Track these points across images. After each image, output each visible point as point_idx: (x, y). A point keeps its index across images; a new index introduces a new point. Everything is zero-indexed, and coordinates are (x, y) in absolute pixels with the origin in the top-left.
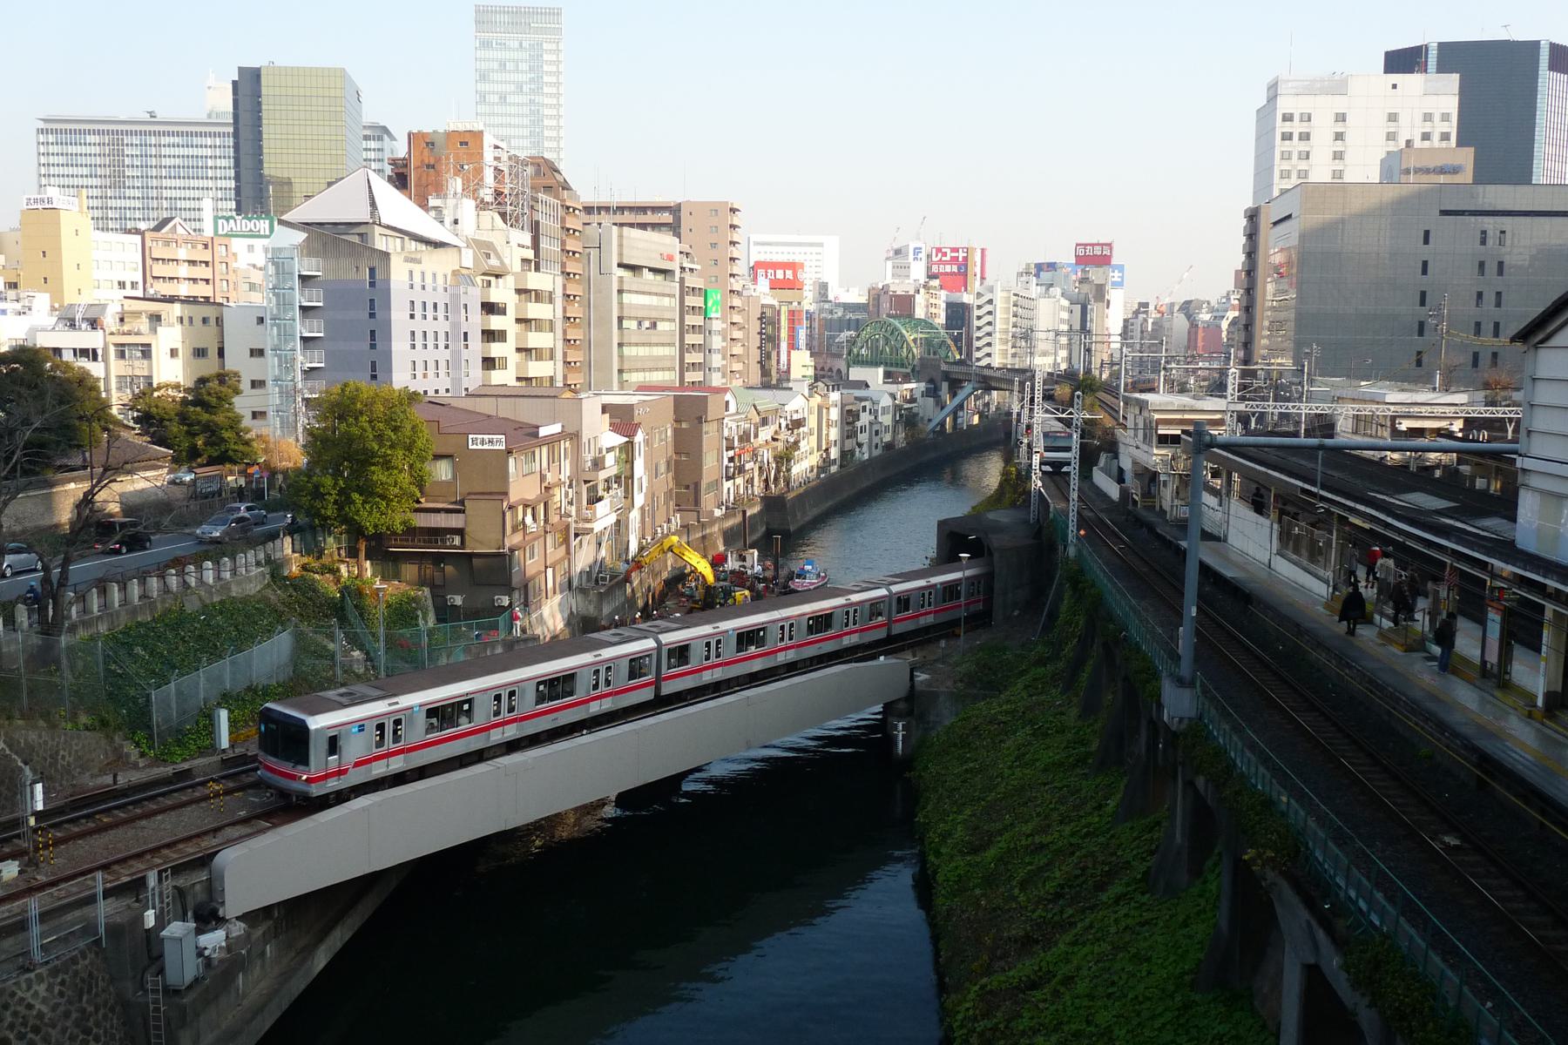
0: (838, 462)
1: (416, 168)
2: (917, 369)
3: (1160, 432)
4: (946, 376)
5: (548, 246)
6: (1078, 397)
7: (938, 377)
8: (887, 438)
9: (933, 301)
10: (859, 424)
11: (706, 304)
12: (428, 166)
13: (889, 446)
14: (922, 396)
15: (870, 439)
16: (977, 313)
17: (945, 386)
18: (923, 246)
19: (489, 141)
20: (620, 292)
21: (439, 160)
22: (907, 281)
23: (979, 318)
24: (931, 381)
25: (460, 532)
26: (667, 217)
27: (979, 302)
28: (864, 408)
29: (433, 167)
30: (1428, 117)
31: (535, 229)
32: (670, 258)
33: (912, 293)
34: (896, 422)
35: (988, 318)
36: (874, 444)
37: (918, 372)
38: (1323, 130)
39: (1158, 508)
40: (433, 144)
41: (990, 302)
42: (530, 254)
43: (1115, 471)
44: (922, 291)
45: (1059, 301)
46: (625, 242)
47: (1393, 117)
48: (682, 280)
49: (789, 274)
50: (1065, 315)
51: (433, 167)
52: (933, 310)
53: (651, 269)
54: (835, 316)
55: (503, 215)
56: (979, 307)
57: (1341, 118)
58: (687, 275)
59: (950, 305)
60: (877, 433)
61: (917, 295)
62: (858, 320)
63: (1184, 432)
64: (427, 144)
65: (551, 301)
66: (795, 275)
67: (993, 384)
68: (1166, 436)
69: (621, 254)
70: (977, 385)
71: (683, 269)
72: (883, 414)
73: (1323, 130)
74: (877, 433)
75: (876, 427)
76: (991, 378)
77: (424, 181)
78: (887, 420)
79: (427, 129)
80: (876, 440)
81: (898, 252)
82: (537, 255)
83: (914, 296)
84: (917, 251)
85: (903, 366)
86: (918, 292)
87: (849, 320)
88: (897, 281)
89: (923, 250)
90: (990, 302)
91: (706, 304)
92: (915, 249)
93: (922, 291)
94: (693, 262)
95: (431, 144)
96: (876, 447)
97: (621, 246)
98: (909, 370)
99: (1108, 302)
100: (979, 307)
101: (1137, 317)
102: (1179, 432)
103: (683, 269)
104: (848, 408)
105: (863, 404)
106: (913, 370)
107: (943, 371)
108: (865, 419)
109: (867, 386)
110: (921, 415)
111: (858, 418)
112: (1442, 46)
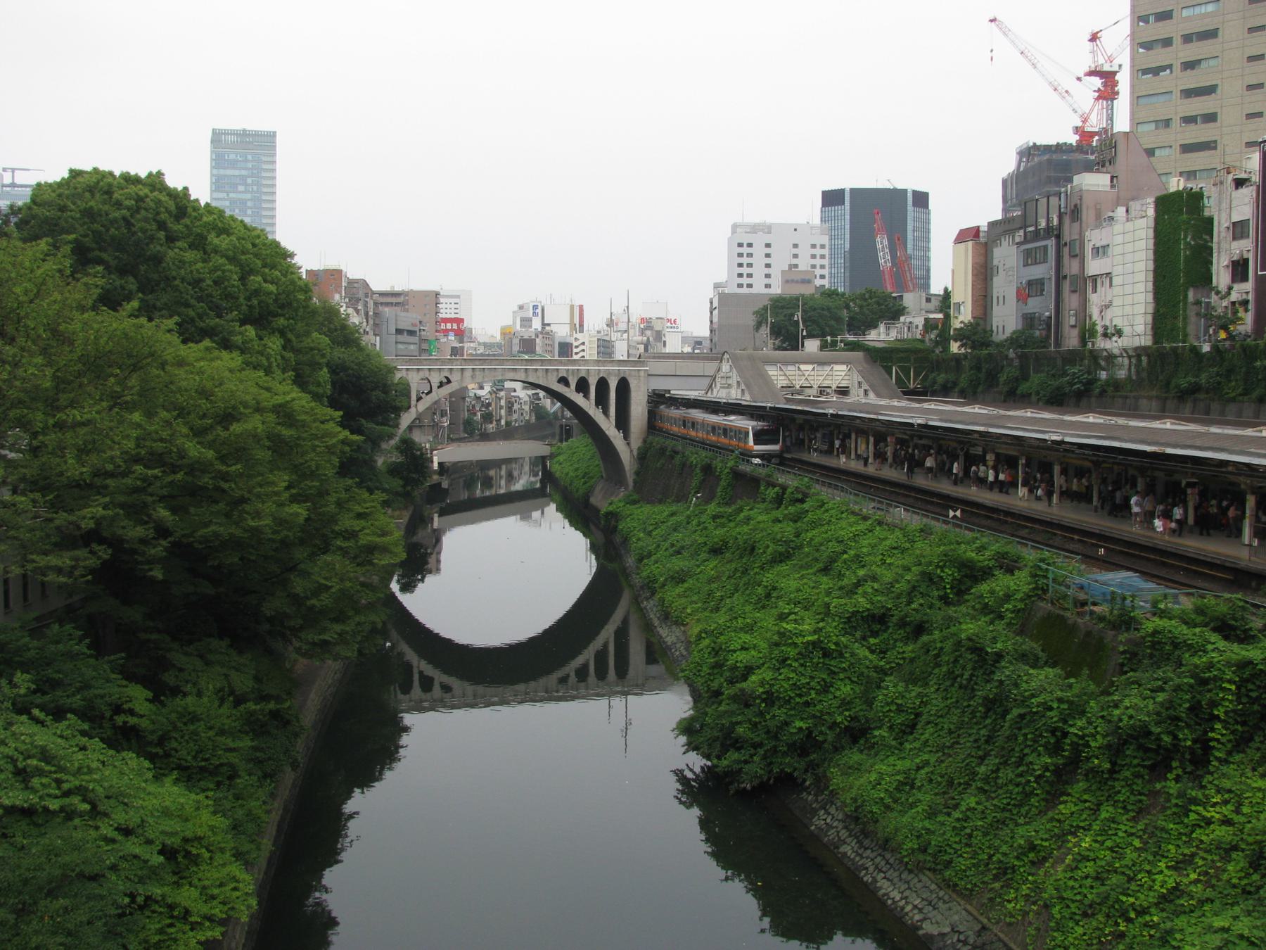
13: (528, 421)
16: (575, 350)
23: (576, 353)
26: (401, 299)
27: (575, 344)
30: (814, 246)
32: (414, 325)
34: (531, 410)
38: (759, 251)
41: (583, 344)
44: (540, 336)
47: (795, 246)
49: (455, 327)
54: (479, 352)
56: (577, 347)
57: (768, 245)
58: (423, 333)
66: (458, 326)
73: (759, 251)
78: (527, 408)
79: (315, 268)
81: (521, 307)
93: (540, 336)
99: (665, 342)
100: (577, 347)
108: (516, 407)
109: (515, 391)
111: (513, 405)
112: (852, 190)
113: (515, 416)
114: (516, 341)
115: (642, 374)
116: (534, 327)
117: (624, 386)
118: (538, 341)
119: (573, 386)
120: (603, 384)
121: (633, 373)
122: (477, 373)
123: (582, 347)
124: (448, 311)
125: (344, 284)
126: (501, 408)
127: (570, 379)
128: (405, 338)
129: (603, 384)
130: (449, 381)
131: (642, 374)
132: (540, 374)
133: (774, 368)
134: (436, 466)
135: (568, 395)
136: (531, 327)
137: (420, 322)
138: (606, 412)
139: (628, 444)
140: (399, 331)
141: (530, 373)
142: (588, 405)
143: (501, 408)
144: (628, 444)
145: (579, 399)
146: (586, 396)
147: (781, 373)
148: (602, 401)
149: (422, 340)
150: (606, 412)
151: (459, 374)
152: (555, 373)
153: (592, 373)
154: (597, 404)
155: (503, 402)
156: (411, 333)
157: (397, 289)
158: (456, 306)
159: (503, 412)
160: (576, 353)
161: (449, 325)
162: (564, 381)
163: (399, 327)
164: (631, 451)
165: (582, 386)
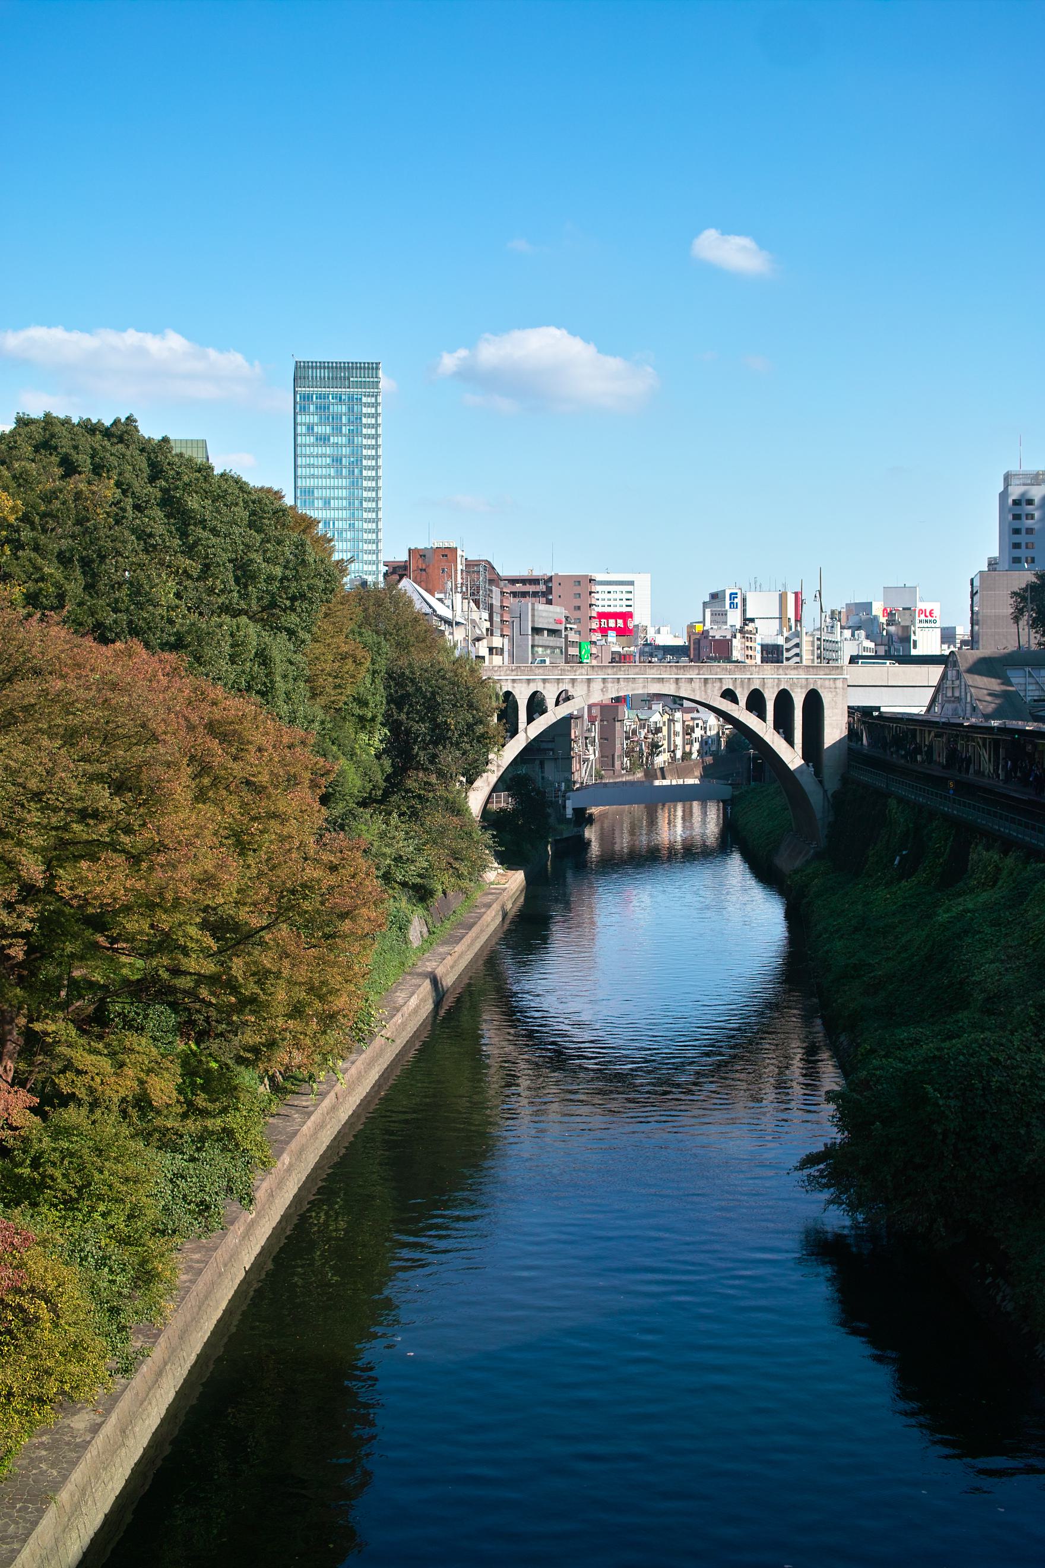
1: (413, 571)
5: (497, 619)
9: (749, 644)
11: (580, 652)
12: (421, 570)
16: (786, 655)
18: (739, 592)
19: (459, 552)
20: (533, 646)
21: (428, 566)
22: (725, 627)
23: (788, 659)
25: (552, 750)
26: (542, 587)
27: (786, 646)
28: (697, 725)
29: (425, 570)
31: (490, 609)
33: (729, 637)
40: (425, 556)
41: (797, 645)
42: (488, 624)
44: (738, 635)
45: (861, 643)
46: (536, 613)
48: (566, 636)
51: (425, 570)
52: (750, 653)
53: (549, 631)
55: (477, 603)
56: (788, 650)
59: (762, 646)
64: (421, 556)
65: (502, 654)
66: (625, 623)
69: (533, 621)
71: (566, 628)
77: (418, 580)
79: (421, 546)
81: (714, 596)
82: (492, 625)
83: (731, 640)
84: (733, 596)
88: (715, 627)
89: (739, 596)
91: (580, 652)
92: (731, 594)
93: (738, 635)
94: (570, 623)
95: (423, 556)
97: (533, 616)
99: (915, 642)
100: (788, 650)
103: (566, 628)
104: (686, 723)
105: (696, 722)
111: (693, 731)
115: (839, 684)
116: (729, 623)
117: (814, 701)
118: (735, 642)
119: (743, 701)
120: (784, 699)
121: (827, 682)
122: (610, 685)
124: (612, 603)
125: (460, 567)
126: (676, 734)
127: (738, 692)
128: (545, 639)
129: (784, 699)
130: (568, 699)
131: (839, 684)
132: (696, 685)
133: (1020, 673)
134: (569, 813)
135: (735, 715)
136: (725, 623)
137: (567, 618)
138: (790, 740)
139: (821, 782)
140: (536, 631)
141: (682, 684)
142: (765, 729)
143: (676, 734)
144: (821, 782)
145: (751, 720)
146: (762, 716)
147: (1031, 680)
148: (783, 725)
149: (568, 644)
150: (790, 740)
151: (585, 687)
152: (718, 685)
153: (769, 683)
154: (777, 727)
155: (678, 727)
156: (553, 632)
157: (537, 573)
158: (629, 596)
159: (679, 741)
160: (788, 659)
161: (612, 623)
162: (729, 695)
163: (536, 626)
164: (825, 791)
165: (756, 703)
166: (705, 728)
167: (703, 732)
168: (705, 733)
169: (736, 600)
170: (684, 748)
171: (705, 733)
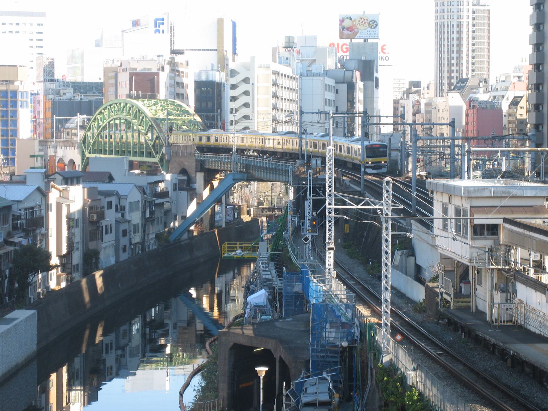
0: (81, 268)
2: (166, 158)
3: (476, 222)
4: (201, 166)
6: (388, 182)
7: (191, 166)
8: (137, 239)
10: (104, 223)
14: (175, 189)
15: (117, 240)
17: (200, 177)
24: (184, 172)
33: (154, 70)
35: (244, 99)
36: (122, 246)
37: (168, 161)
39: (473, 309)
41: (246, 80)
43: (412, 269)
50: (330, 96)
54: (64, 98)
56: (234, 87)
60: (125, 233)
61: (161, 73)
62: (90, 102)
63: (506, 220)
67: (256, 174)
68: (482, 226)
70: (238, 176)
72: (131, 210)
74: (125, 233)
75: (123, 227)
76: (255, 167)
78: (136, 218)
80: (124, 241)
83: (157, 74)
85: (149, 154)
86: (163, 69)
87: (81, 102)
89: (165, 22)
90: (246, 80)
92: (156, 20)
96: (124, 250)
98: (156, 160)
99: (377, 79)
100: (234, 87)
101: (408, 97)
102: (500, 222)
105: (108, 199)
106: (161, 160)
107: (197, 161)
108: (111, 216)
109: (111, 179)
110: (174, 211)
111: (102, 216)
113: (109, 239)
114: (124, 78)
123: (243, 87)
166: (123, 208)
167: (119, 215)
168: (123, 215)
169: (162, 28)
170: (85, 245)
171: (123, 215)
